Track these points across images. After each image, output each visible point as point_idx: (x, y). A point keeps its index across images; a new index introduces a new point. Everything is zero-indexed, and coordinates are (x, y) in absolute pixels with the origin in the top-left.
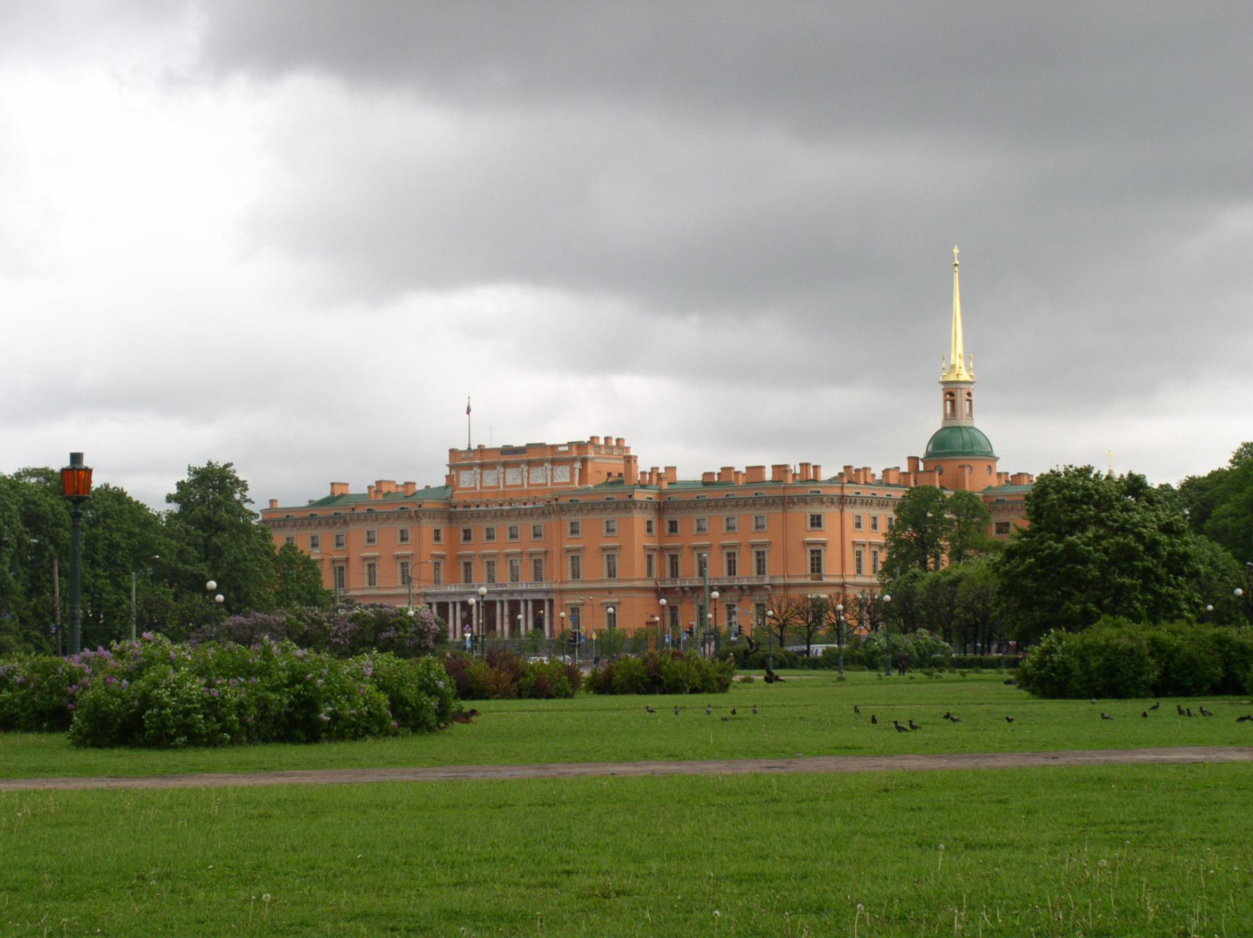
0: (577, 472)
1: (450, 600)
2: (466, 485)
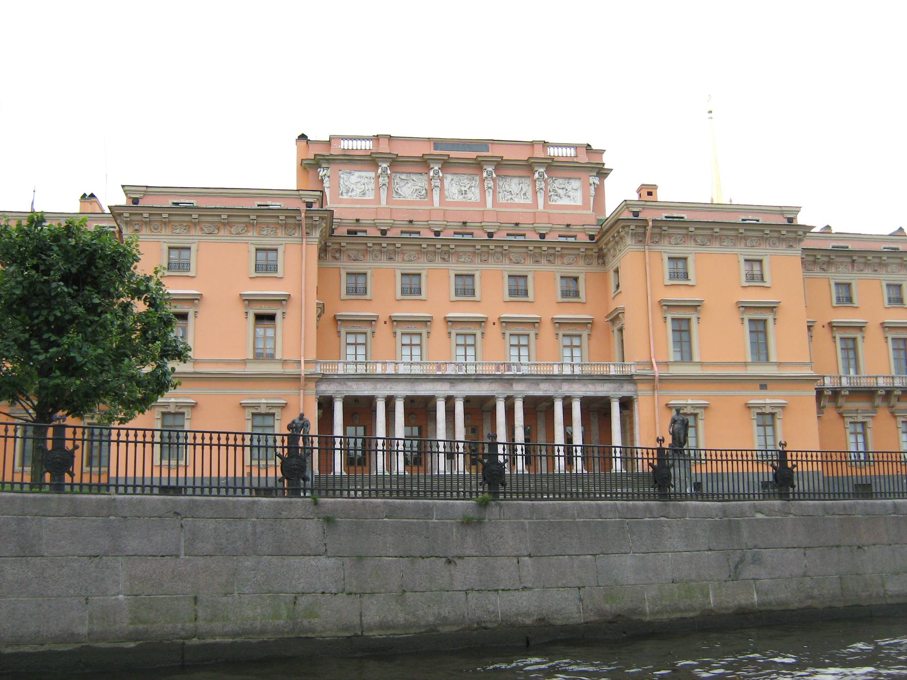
0: (592, 188)
1: (381, 391)
2: (356, 194)
